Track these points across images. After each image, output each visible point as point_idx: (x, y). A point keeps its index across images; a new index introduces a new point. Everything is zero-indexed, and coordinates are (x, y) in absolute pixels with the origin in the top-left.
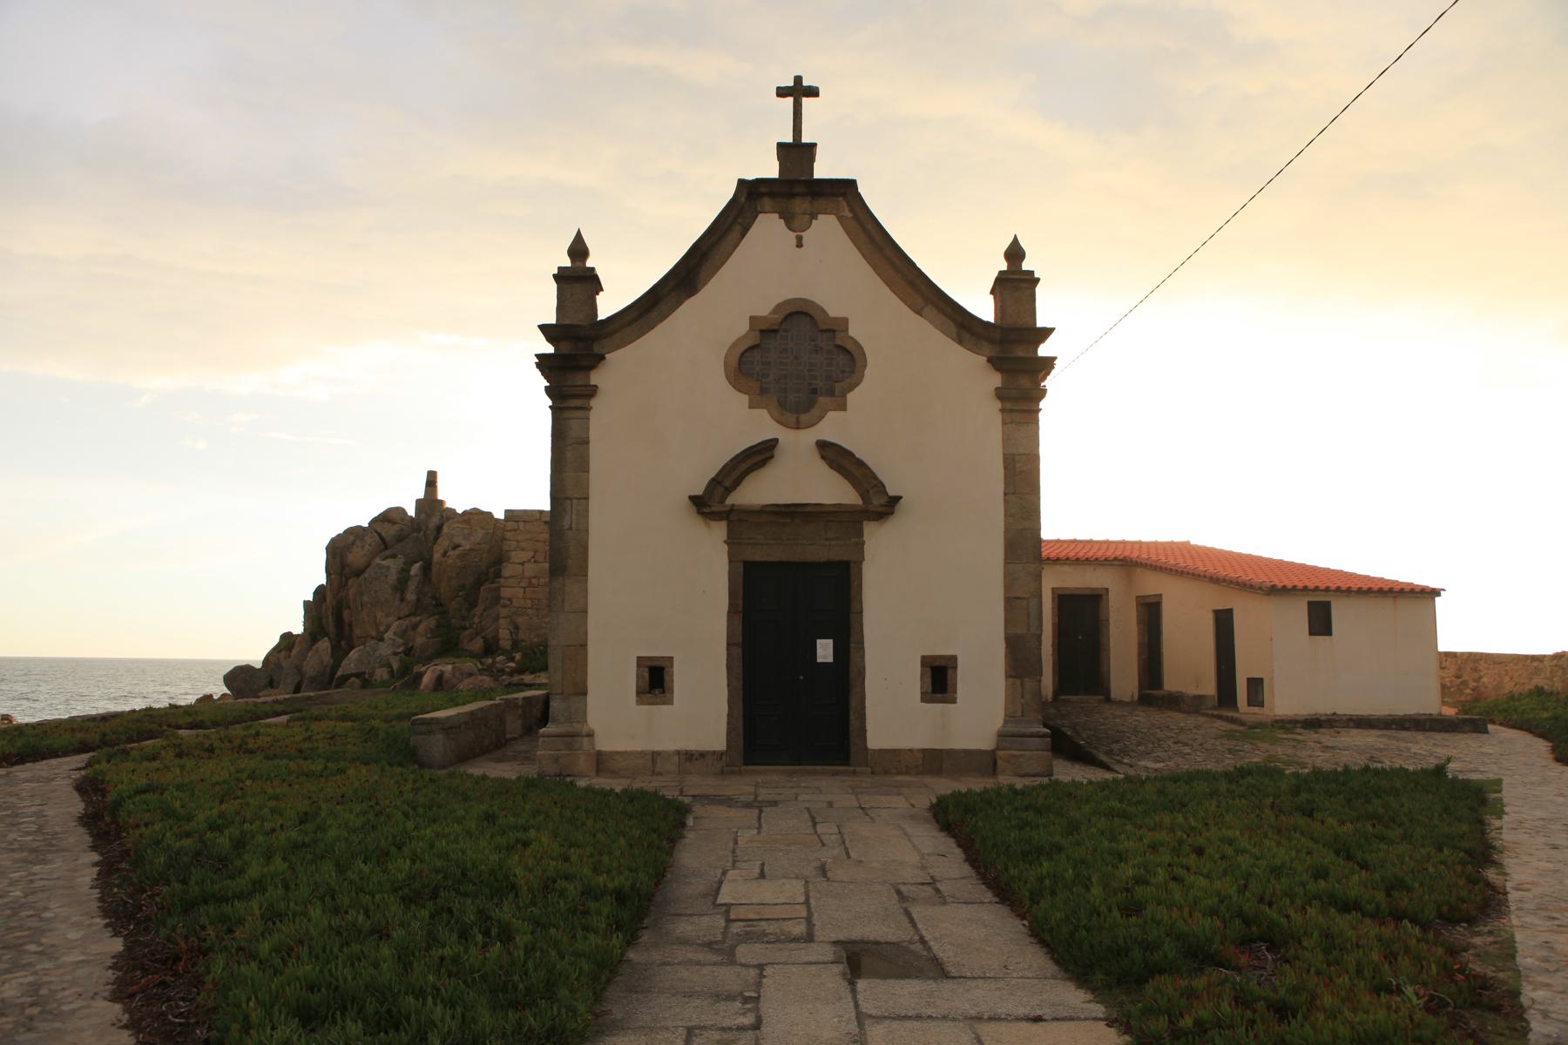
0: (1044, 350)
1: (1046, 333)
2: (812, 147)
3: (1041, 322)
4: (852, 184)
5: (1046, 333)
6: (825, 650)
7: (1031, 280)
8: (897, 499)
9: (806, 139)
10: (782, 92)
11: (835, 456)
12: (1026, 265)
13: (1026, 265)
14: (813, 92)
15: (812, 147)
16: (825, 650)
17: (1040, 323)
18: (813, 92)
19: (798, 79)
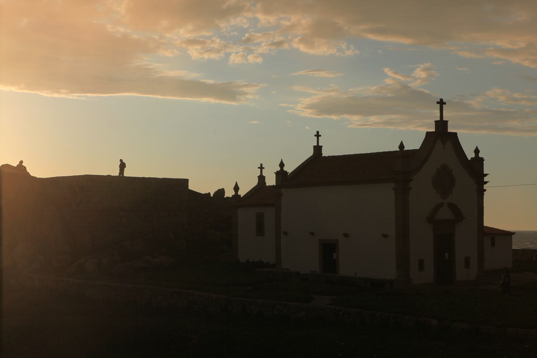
0: (486, 179)
1: (486, 175)
2: (446, 122)
3: (485, 173)
4: (455, 134)
5: (486, 175)
6: (447, 255)
7: (482, 160)
8: (464, 218)
9: (444, 119)
10: (438, 103)
11: (453, 207)
12: (480, 155)
13: (480, 155)
14: (445, 103)
15: (447, 122)
16: (447, 255)
17: (485, 173)
18: (445, 103)
19: (441, 100)
